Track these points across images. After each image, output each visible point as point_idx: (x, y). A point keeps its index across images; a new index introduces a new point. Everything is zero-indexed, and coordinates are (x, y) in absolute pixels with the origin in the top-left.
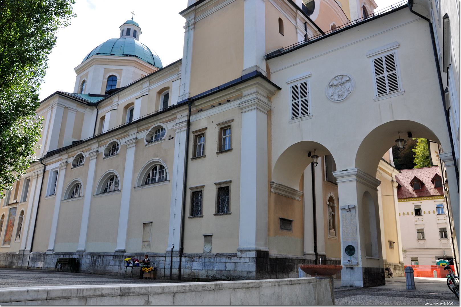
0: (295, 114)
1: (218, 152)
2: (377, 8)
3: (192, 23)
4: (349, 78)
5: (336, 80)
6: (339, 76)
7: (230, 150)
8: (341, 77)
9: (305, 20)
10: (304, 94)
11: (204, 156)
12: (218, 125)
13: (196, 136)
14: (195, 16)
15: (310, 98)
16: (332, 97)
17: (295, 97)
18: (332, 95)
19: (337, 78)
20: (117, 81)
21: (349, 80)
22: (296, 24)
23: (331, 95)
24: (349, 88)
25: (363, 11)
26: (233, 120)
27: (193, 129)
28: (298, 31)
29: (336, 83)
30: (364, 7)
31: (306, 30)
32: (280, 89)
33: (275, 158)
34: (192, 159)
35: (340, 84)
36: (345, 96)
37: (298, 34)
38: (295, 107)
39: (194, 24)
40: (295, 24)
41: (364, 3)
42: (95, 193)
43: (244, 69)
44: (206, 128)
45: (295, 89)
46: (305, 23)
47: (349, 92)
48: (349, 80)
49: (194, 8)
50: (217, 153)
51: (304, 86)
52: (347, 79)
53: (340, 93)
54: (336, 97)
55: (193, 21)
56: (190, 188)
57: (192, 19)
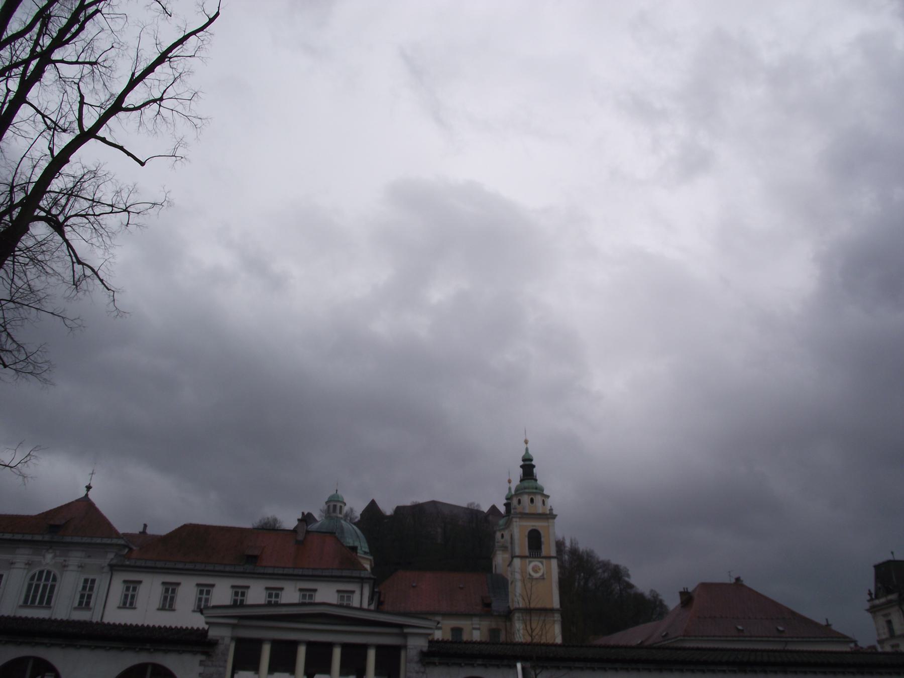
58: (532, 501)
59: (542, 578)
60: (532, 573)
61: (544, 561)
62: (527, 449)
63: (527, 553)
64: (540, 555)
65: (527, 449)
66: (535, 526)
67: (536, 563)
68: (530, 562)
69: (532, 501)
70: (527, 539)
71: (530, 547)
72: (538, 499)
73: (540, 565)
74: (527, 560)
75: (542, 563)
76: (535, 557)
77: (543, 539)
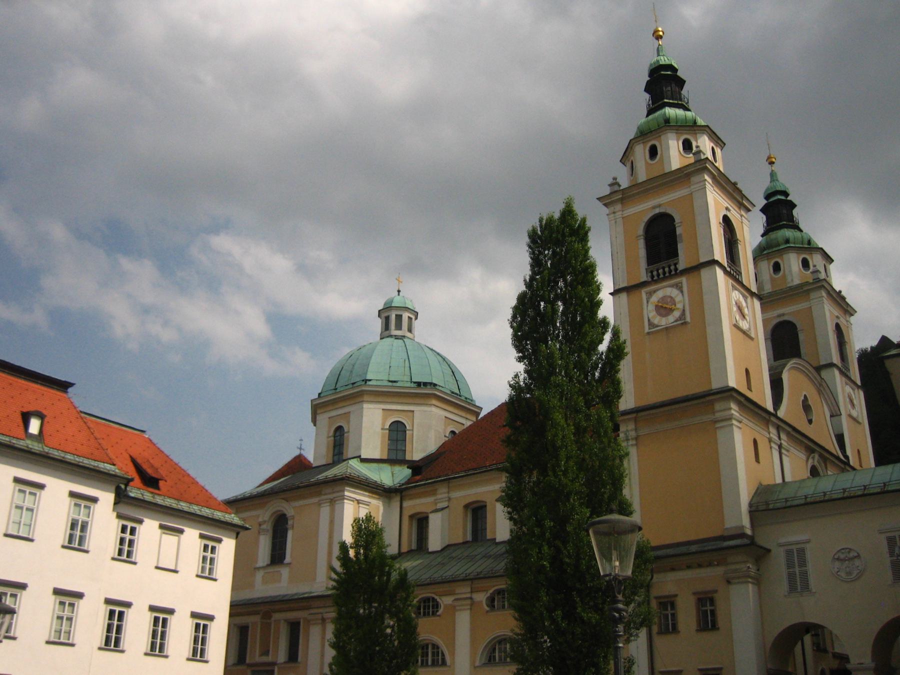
0: (792, 588)
1: (698, 629)
2: (856, 315)
3: (633, 437)
4: (858, 553)
5: (843, 553)
6: (846, 549)
7: (714, 627)
8: (847, 550)
9: (777, 424)
10: (803, 563)
11: (675, 630)
12: (694, 594)
13: (660, 603)
14: (636, 426)
15: (810, 568)
16: (838, 574)
17: (790, 564)
18: (839, 571)
19: (843, 551)
20: (407, 432)
21: (858, 556)
22: (769, 433)
23: (836, 570)
24: (858, 566)
25: (836, 336)
26: (716, 591)
28: (773, 445)
29: (842, 556)
30: (838, 326)
31: (779, 438)
32: (769, 551)
33: (770, 639)
34: (660, 633)
35: (847, 559)
36: (854, 575)
37: (773, 449)
38: (791, 578)
39: (636, 438)
40: (768, 436)
41: (838, 317)
42: (477, 664)
43: (727, 525)
44: (676, 596)
45: (789, 553)
46: (778, 428)
47: (859, 571)
48: (858, 556)
49: (634, 415)
50: (697, 630)
51: (802, 552)
52: (856, 554)
53: (848, 569)
54: (843, 574)
55: (633, 434)
57: (631, 430)
59: (682, 322)
60: (657, 320)
61: (684, 280)
64: (676, 269)
66: (659, 206)
67: (666, 291)
68: (650, 294)
70: (641, 243)
73: (674, 292)
74: (644, 292)
75: (679, 287)
76: (659, 280)
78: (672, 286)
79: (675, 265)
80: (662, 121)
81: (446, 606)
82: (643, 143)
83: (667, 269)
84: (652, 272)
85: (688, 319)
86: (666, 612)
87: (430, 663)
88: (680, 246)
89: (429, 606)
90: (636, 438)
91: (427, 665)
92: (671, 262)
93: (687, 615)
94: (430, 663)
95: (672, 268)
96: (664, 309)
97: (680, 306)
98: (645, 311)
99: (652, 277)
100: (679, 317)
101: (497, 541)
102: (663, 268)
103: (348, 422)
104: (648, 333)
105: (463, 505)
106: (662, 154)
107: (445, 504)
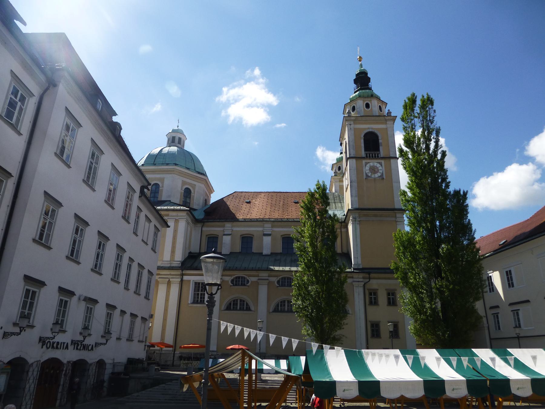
12: (386, 290)
27: (367, 286)
39: (359, 221)
44: (378, 290)
56: (370, 322)
58: (367, 106)
59: (381, 177)
61: (383, 162)
62: (361, 66)
63: (363, 153)
64: (378, 156)
65: (361, 66)
66: (372, 129)
67: (374, 163)
68: (366, 164)
69: (367, 106)
71: (366, 149)
72: (374, 104)
73: (378, 165)
74: (364, 161)
77: (380, 141)
78: (377, 162)
79: (378, 154)
80: (370, 95)
81: (252, 282)
82: (363, 100)
83: (374, 155)
84: (367, 154)
85: (384, 177)
86: (371, 296)
87: (238, 308)
88: (381, 148)
89: (239, 281)
90: (359, 221)
91: (236, 310)
92: (376, 152)
93: (382, 298)
94: (238, 308)
95: (376, 155)
96: (373, 170)
97: (381, 171)
98: (364, 170)
99: (367, 156)
100: (380, 176)
101: (263, 254)
102: (372, 154)
103: (163, 183)
104: (366, 179)
105: (240, 235)
106: (372, 108)
107: (230, 233)
